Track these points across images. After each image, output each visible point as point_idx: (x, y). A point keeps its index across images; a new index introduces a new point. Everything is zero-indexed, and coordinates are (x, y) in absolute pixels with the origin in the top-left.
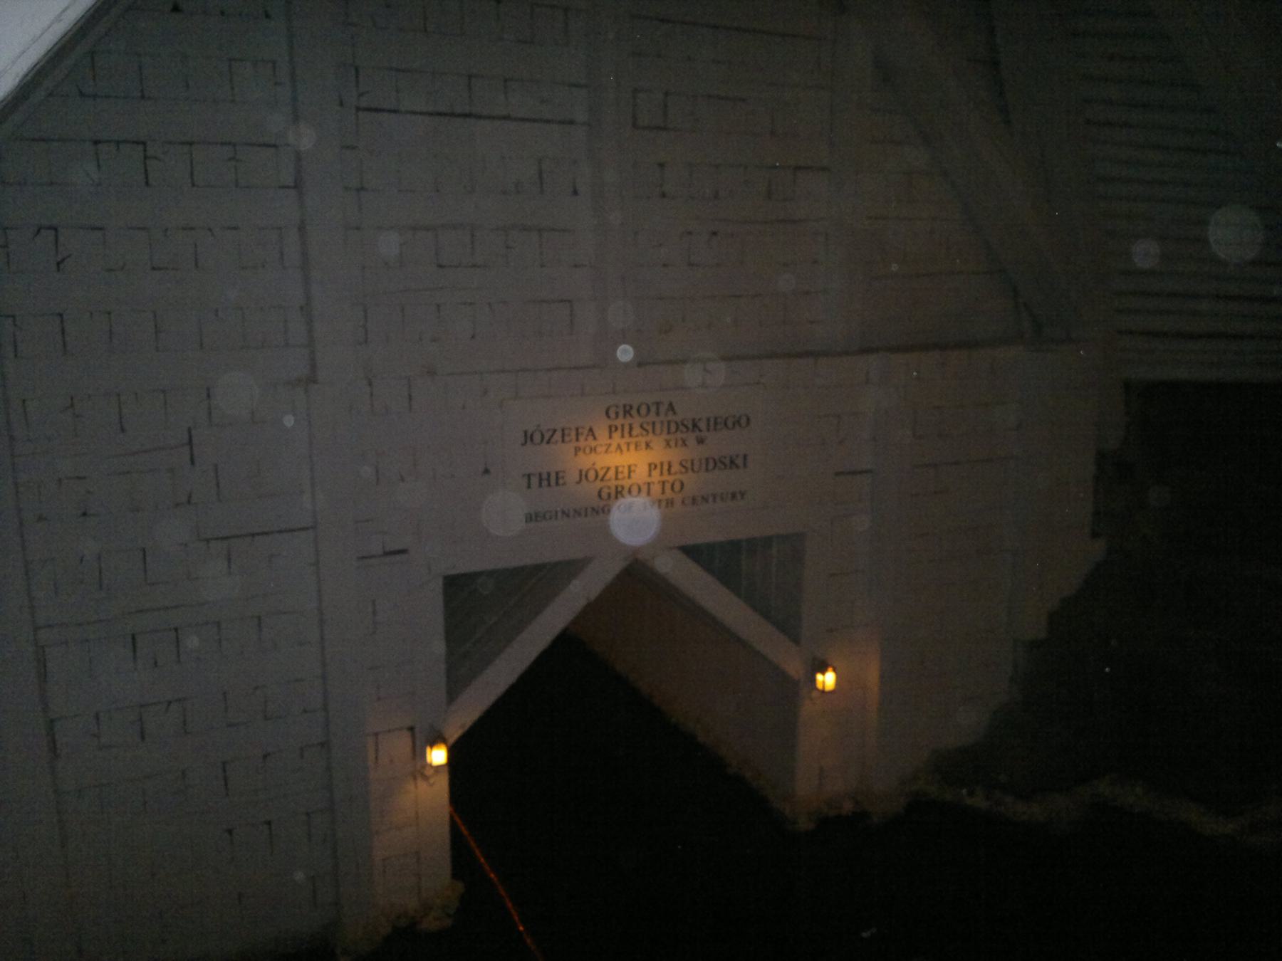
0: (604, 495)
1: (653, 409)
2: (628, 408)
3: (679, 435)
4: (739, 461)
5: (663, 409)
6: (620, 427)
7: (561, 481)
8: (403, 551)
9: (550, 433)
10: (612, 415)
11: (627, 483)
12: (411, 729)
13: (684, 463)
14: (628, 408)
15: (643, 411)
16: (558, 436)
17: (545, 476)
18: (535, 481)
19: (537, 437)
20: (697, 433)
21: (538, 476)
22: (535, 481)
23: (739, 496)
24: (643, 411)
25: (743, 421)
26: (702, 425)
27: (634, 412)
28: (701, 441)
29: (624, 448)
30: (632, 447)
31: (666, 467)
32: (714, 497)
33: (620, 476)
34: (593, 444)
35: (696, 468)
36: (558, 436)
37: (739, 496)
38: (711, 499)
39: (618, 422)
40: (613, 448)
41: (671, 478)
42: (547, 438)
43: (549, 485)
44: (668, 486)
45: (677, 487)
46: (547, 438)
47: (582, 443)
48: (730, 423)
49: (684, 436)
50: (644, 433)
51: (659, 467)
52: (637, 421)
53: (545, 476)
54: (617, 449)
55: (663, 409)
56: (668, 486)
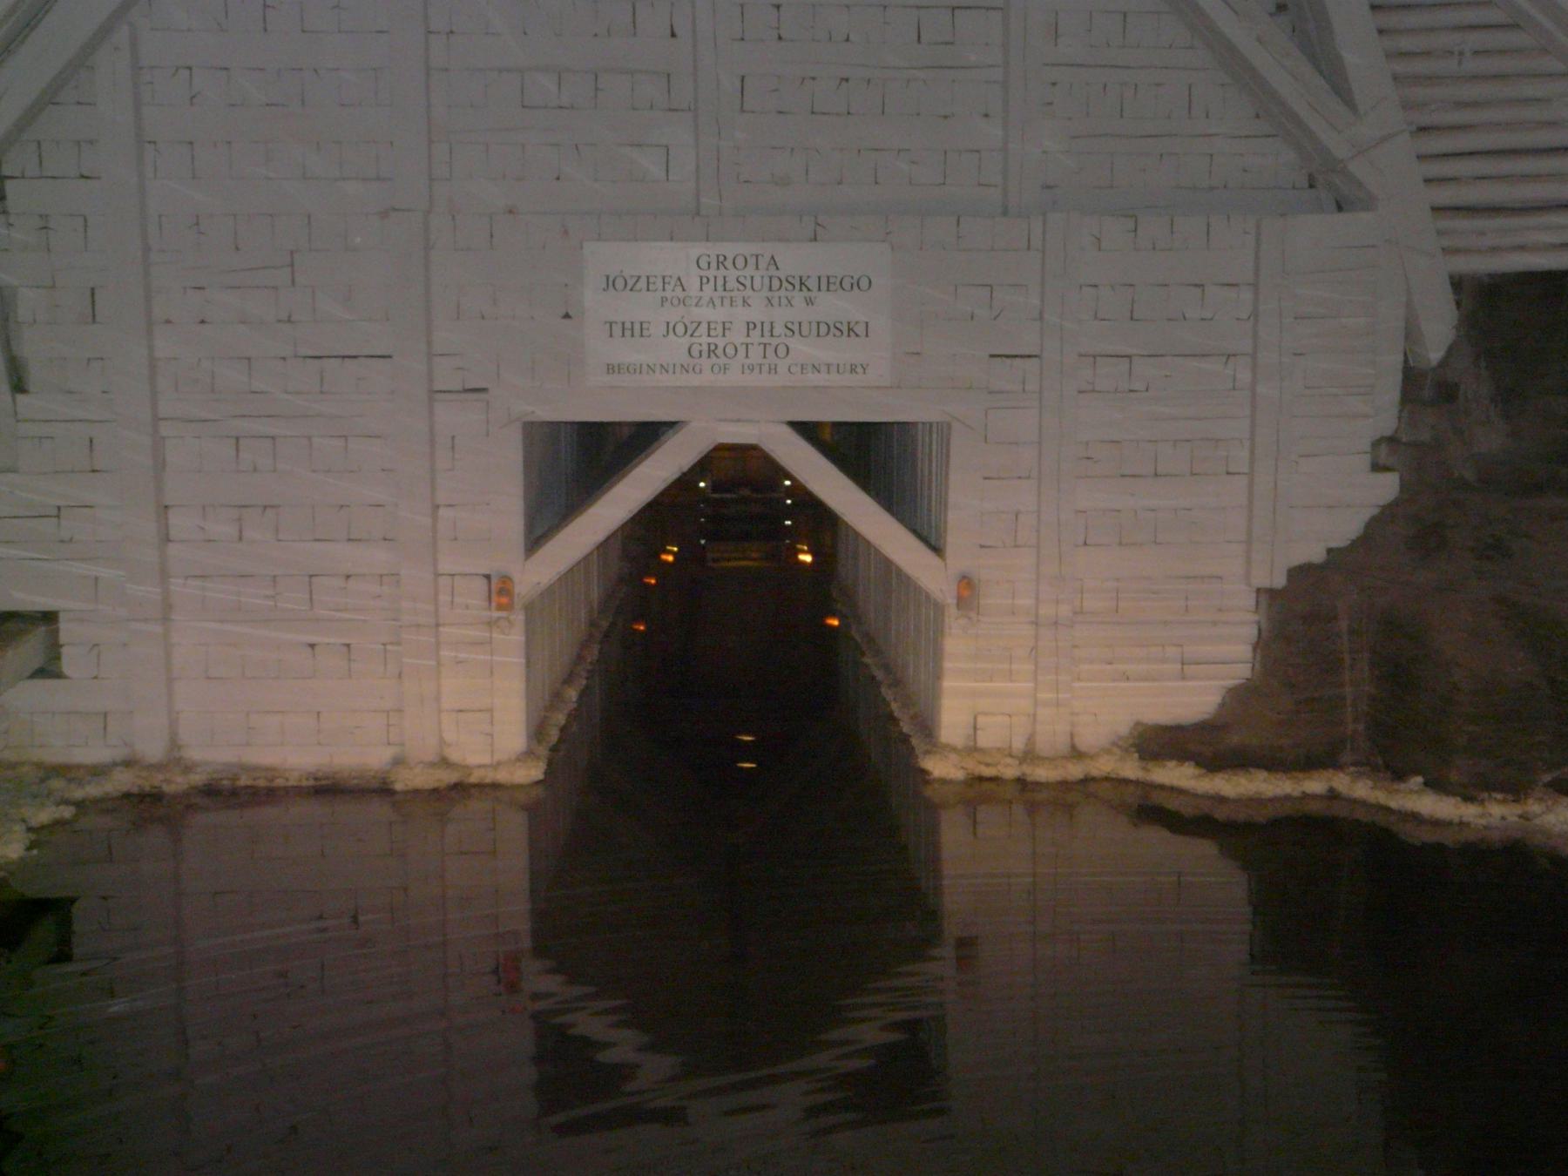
0: (695, 353)
1: (752, 261)
2: (721, 259)
3: (782, 293)
4: (860, 329)
5: (763, 263)
6: (712, 280)
7: (645, 333)
9: (634, 280)
10: (703, 264)
11: (721, 342)
13: (789, 325)
14: (721, 259)
15: (740, 262)
16: (642, 284)
17: (628, 325)
18: (617, 330)
19: (620, 283)
20: (805, 293)
21: (620, 325)
22: (617, 330)
23: (859, 370)
24: (740, 262)
25: (864, 283)
26: (812, 283)
27: (729, 263)
28: (809, 302)
29: (718, 302)
30: (727, 302)
31: (767, 328)
32: (829, 366)
33: (712, 333)
35: (805, 331)
36: (642, 284)
37: (859, 370)
38: (824, 369)
39: (711, 273)
41: (774, 341)
42: (630, 283)
43: (633, 336)
44: (770, 351)
46: (630, 283)
47: (668, 294)
48: (846, 285)
49: (789, 294)
50: (741, 288)
51: (759, 326)
52: (732, 274)
53: (628, 325)
54: (709, 303)
55: (763, 263)
56: (770, 351)
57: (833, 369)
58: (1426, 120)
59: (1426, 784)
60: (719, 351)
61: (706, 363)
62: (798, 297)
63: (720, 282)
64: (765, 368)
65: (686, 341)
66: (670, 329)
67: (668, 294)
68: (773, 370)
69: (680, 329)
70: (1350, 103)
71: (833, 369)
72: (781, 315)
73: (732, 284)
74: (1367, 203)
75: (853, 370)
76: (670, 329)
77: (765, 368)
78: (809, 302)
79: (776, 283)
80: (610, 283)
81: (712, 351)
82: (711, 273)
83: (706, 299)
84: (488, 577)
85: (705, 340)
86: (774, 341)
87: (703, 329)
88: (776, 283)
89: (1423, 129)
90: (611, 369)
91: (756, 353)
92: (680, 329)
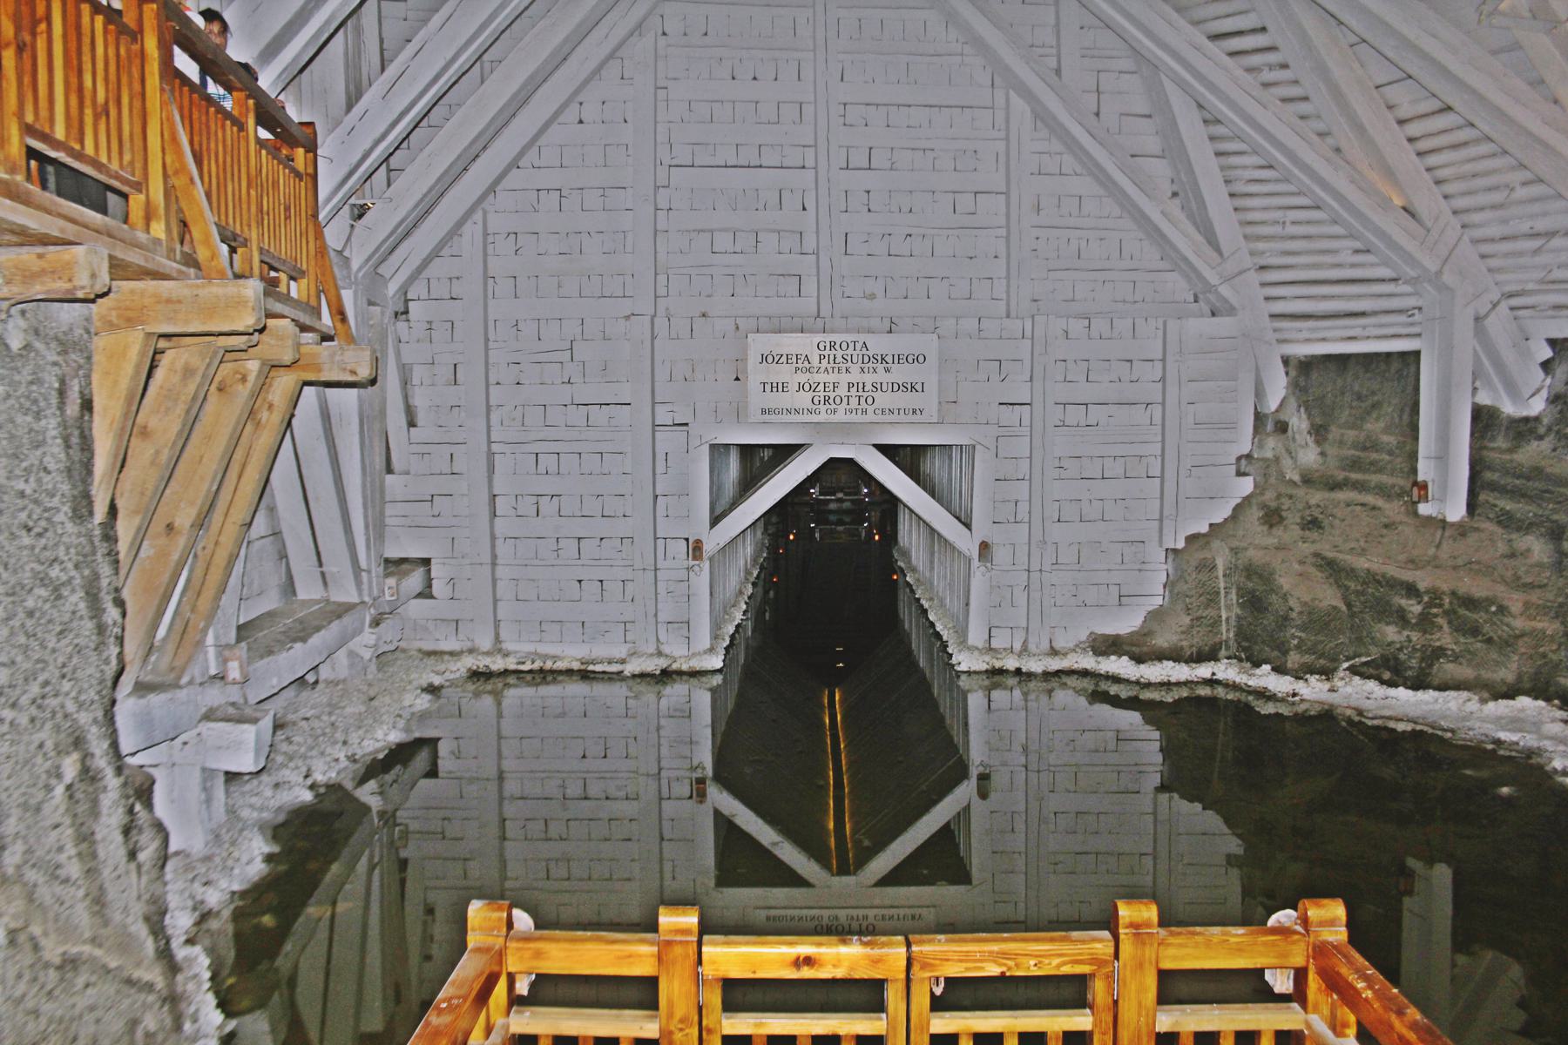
0: (816, 401)
1: (851, 345)
3: (870, 364)
4: (918, 387)
5: (858, 346)
8: (686, 424)
10: (822, 347)
11: (832, 395)
12: (687, 540)
16: (784, 359)
18: (768, 387)
19: (770, 359)
20: (885, 365)
22: (768, 387)
25: (921, 359)
26: (889, 359)
27: (837, 347)
31: (861, 386)
34: (808, 366)
35: (884, 388)
36: (784, 359)
38: (896, 412)
39: (827, 352)
40: (822, 370)
41: (865, 395)
44: (863, 400)
45: (870, 400)
48: (910, 360)
55: (858, 346)
56: (863, 400)
57: (902, 412)
58: (1263, 262)
59: (1273, 669)
60: (831, 401)
61: (823, 408)
62: (880, 367)
63: (832, 358)
64: (860, 412)
65: (811, 394)
66: (801, 387)
67: (800, 366)
68: (865, 412)
69: (807, 387)
70: (1219, 251)
71: (902, 412)
72: (869, 379)
73: (839, 359)
74: (1231, 311)
75: (914, 412)
76: (801, 387)
77: (860, 412)
78: (887, 370)
79: (866, 359)
80: (764, 358)
81: (826, 401)
82: (827, 352)
83: (822, 370)
84: (687, 540)
85: (822, 394)
86: (865, 395)
87: (821, 387)
88: (866, 359)
89: (1262, 268)
90: (764, 412)
91: (854, 401)
92: (807, 387)
